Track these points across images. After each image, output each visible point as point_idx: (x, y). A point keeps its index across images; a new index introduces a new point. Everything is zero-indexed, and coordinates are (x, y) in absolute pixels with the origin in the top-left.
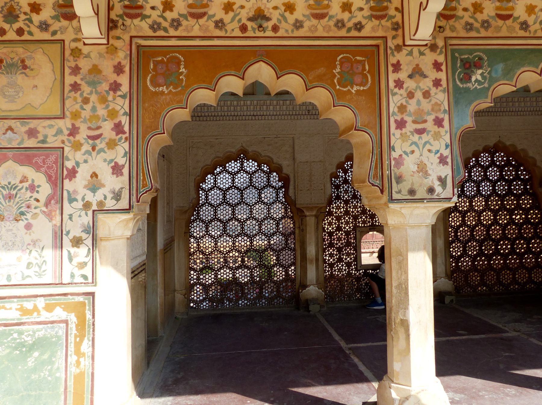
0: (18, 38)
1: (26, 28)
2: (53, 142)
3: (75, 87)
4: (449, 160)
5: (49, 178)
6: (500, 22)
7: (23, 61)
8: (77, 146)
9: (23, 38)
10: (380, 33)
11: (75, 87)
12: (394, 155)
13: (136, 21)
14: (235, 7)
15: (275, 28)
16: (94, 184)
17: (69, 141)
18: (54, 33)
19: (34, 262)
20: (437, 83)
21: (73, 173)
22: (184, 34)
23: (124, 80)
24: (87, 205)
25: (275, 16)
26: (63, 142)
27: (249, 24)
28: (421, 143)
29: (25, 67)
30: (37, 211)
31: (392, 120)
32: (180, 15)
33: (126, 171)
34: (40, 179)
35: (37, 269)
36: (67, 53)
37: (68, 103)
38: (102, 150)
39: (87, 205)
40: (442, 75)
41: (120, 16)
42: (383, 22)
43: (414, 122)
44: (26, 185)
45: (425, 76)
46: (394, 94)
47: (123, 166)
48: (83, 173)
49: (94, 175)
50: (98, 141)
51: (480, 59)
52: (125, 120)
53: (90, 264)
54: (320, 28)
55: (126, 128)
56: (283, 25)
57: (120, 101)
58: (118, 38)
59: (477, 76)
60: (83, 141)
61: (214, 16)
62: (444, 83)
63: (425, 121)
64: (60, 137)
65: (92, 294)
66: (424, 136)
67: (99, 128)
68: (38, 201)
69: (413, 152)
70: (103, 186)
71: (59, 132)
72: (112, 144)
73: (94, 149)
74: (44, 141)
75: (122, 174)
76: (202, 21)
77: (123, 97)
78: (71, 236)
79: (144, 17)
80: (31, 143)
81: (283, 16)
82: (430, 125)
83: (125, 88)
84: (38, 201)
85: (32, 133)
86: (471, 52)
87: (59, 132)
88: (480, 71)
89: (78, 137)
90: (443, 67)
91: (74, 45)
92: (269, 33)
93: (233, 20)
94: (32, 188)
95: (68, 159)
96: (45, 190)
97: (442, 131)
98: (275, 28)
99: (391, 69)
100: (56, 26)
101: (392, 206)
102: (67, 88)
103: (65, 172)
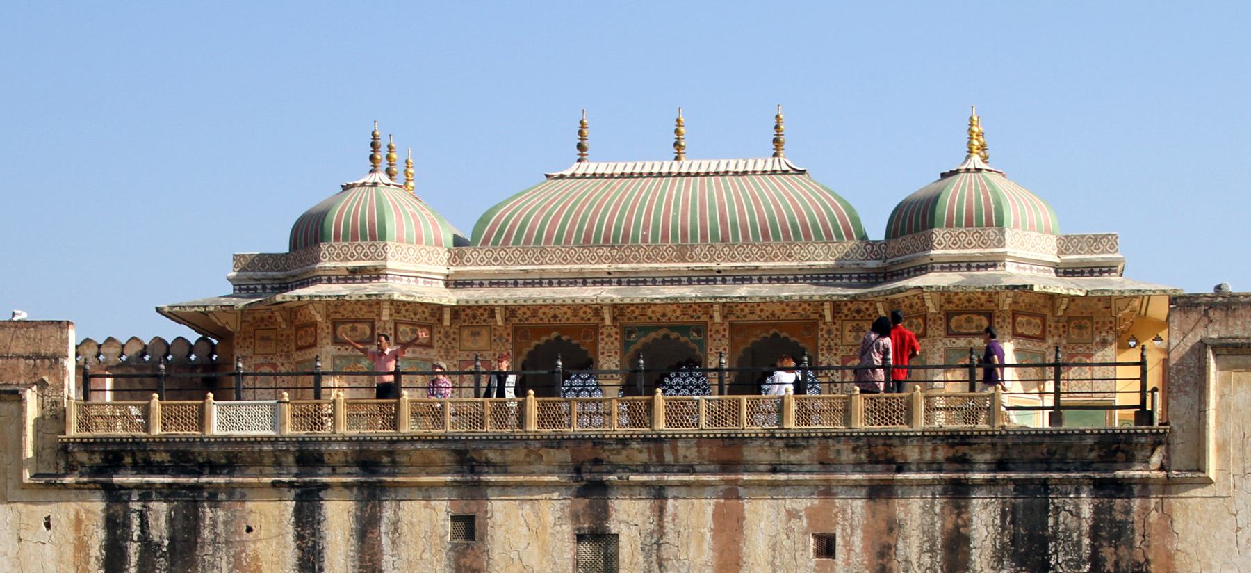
23: (510, 338)
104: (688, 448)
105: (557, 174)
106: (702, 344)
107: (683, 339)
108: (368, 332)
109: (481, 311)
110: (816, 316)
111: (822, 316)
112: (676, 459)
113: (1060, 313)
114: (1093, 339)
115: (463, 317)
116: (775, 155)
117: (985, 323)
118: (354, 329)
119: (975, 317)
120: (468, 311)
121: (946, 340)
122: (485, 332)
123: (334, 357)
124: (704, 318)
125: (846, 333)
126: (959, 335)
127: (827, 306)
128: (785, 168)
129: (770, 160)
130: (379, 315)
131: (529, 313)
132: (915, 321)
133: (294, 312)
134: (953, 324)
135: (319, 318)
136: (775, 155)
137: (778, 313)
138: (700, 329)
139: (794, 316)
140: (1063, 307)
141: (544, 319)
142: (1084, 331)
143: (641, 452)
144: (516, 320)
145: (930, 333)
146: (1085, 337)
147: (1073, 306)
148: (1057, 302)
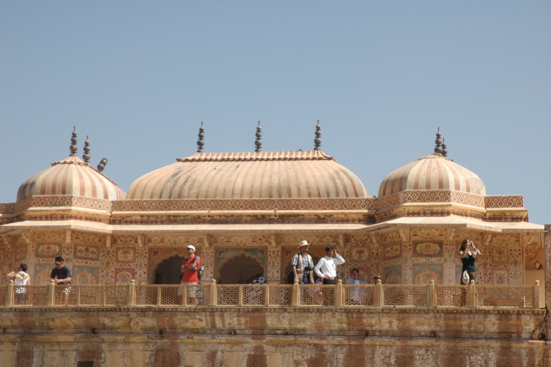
2: (133, 267)
3: (138, 257)
8: (137, 268)
20: (212, 256)
21: (136, 274)
23: (147, 255)
25: (178, 242)
40: (213, 255)
52: (147, 263)
59: (222, 254)
72: (144, 268)
80: (129, 267)
82: (209, 265)
85: (129, 265)
104: (231, 319)
105: (184, 159)
106: (265, 259)
107: (253, 257)
108: (58, 250)
109: (130, 238)
110: (335, 244)
111: (338, 243)
112: (224, 325)
113: (487, 244)
114: (508, 260)
115: (119, 242)
116: (315, 149)
117: (437, 248)
118: (49, 248)
119: (432, 245)
120: (122, 238)
121: (414, 259)
122: (131, 251)
123: (36, 265)
124: (266, 244)
126: (421, 255)
127: (341, 237)
128: (321, 156)
129: (311, 152)
130: (65, 239)
131: (159, 240)
132: (395, 247)
133: (15, 238)
134: (418, 248)
135: (28, 241)
136: (315, 149)
138: (263, 250)
139: (321, 244)
140: (489, 240)
141: (167, 243)
142: (502, 255)
143: (201, 320)
144: (151, 244)
145: (403, 255)
146: (503, 259)
147: (495, 240)
148: (485, 236)
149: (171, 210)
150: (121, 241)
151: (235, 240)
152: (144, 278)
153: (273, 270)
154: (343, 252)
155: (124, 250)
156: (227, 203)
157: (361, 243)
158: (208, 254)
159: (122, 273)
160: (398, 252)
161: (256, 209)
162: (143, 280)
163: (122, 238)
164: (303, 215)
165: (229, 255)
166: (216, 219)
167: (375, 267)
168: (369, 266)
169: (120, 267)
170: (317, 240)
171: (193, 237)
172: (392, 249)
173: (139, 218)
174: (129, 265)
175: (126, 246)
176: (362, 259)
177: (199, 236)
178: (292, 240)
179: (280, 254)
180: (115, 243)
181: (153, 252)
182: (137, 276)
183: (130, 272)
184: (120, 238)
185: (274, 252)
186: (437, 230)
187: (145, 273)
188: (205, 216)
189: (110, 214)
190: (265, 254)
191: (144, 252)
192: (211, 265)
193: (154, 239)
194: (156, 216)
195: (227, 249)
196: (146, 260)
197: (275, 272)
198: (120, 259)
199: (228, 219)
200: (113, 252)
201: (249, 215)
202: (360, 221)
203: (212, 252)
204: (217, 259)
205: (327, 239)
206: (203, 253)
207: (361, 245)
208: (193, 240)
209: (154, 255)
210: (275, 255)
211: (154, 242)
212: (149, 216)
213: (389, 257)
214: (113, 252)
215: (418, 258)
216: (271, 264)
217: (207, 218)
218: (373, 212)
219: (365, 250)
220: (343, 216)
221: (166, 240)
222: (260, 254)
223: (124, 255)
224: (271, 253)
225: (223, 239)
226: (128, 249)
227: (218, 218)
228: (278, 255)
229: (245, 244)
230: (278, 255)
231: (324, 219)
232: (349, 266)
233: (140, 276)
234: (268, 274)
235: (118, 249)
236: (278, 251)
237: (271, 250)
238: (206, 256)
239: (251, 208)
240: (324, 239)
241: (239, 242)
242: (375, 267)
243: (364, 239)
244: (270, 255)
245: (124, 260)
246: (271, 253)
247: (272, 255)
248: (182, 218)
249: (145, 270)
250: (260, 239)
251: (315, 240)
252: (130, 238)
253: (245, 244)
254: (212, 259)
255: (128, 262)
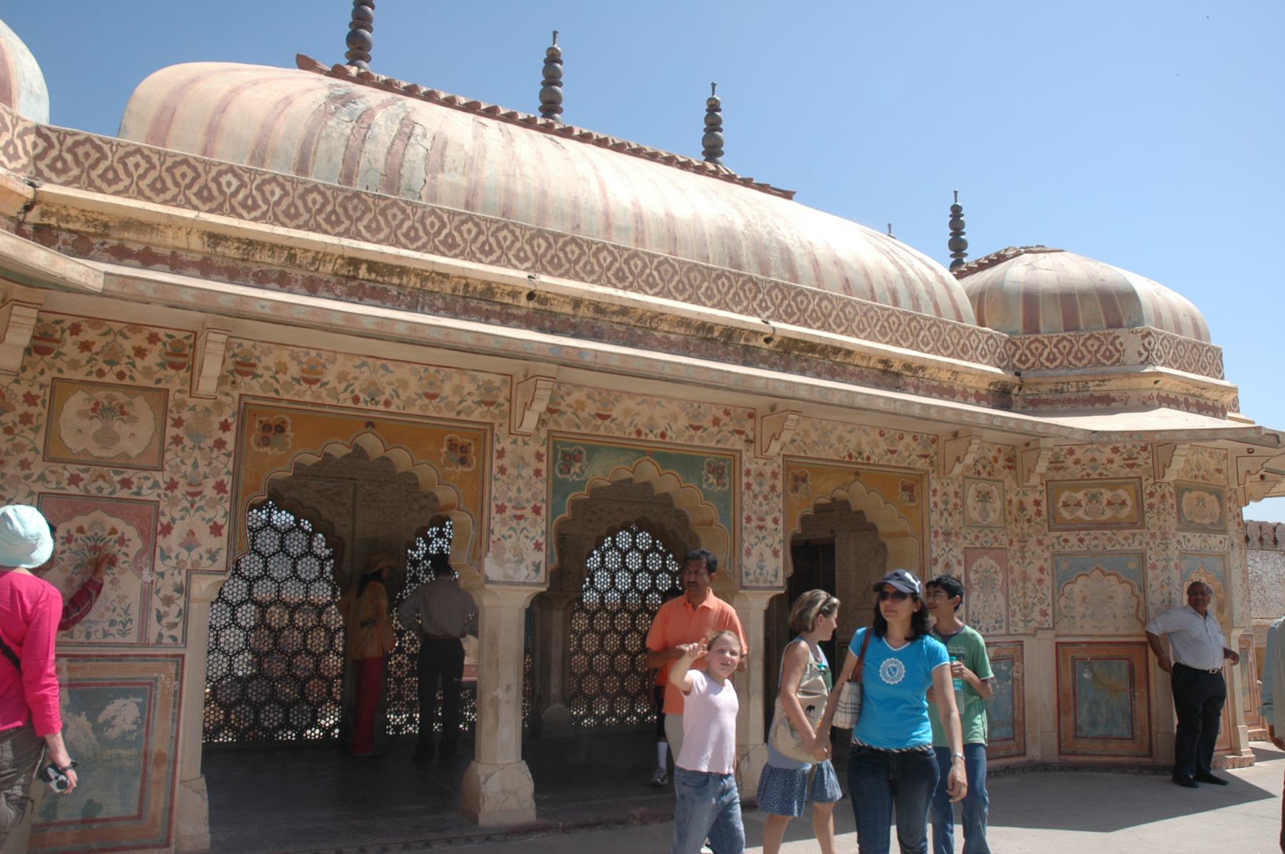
0: (119, 382)
1: (128, 373)
2: (148, 494)
3: (177, 440)
4: (544, 547)
5: (142, 534)
6: (599, 422)
7: (121, 407)
8: (174, 503)
9: (123, 382)
10: (488, 420)
11: (177, 440)
12: (493, 538)
13: (247, 379)
14: (350, 377)
15: (387, 403)
16: (190, 542)
17: (166, 495)
18: (158, 381)
19: (118, 619)
20: (538, 473)
21: (167, 530)
22: (296, 398)
23: (229, 437)
24: (180, 564)
25: (388, 391)
26: (159, 496)
27: (362, 396)
28: (518, 529)
29: (123, 413)
30: (126, 566)
31: (493, 504)
32: (293, 379)
33: (225, 531)
34: (130, 532)
35: (121, 627)
36: (171, 404)
37: (168, 456)
38: (200, 508)
39: (180, 564)
40: (543, 466)
41: (231, 372)
42: (492, 409)
43: (514, 508)
44: (115, 537)
45: (528, 465)
46: (497, 480)
47: (222, 527)
48: (179, 531)
49: (191, 533)
50: (197, 499)
51: (580, 452)
53: (181, 625)
54: (431, 407)
55: (229, 488)
56: (395, 401)
57: (223, 459)
58: (227, 394)
59: (576, 468)
60: (180, 496)
61: (327, 383)
62: (544, 473)
63: (524, 508)
64: (157, 491)
65: (183, 656)
66: (522, 522)
67: (200, 484)
68: (127, 555)
69: (510, 537)
70: (200, 545)
71: (156, 485)
72: (213, 504)
73: (192, 506)
74: (138, 493)
75: (220, 535)
76: (315, 387)
77: (228, 455)
78: (161, 594)
79: (256, 376)
80: (124, 493)
81: (395, 391)
82: (528, 512)
83: (230, 446)
84: (127, 555)
85: (126, 483)
86: (571, 445)
87: (156, 485)
88: (579, 464)
89: (176, 492)
90: (545, 458)
91: (178, 396)
92: (381, 407)
93: (346, 389)
94: (122, 541)
95: (164, 514)
96: (136, 544)
97: (539, 519)
98: (387, 403)
99: (495, 455)
100: (161, 374)
101: (487, 586)
102: (168, 440)
103: (159, 528)
106: (728, 502)
109: (140, 340)
115: (70, 348)
120: (88, 334)
122: (140, 406)
124: (737, 443)
125: (970, 502)
131: (294, 370)
137: (867, 449)
139: (893, 460)
141: (333, 392)
144: (252, 386)
145: (1152, 520)
149: (358, 236)
150: (85, 346)
151: (627, 412)
152: (213, 557)
153: (761, 547)
154: (945, 494)
155: (101, 395)
156: (595, 255)
157: (984, 467)
158: (521, 462)
159: (80, 520)
160: (1125, 513)
161: (698, 302)
162: (206, 564)
163: (88, 334)
164: (849, 353)
165: (600, 473)
166: (557, 314)
167: (1016, 545)
168: (1005, 541)
169: (73, 490)
170: (883, 445)
171: (456, 378)
172: (1094, 498)
173: (196, 243)
174: (126, 483)
175: (111, 378)
176: (989, 520)
177: (482, 377)
178: (814, 436)
179: (779, 483)
180: (42, 351)
181: (263, 423)
182: (172, 542)
183: (129, 521)
184: (75, 329)
185: (760, 475)
186: (1115, 450)
187: (216, 530)
188: (514, 294)
189: (28, 192)
190: (727, 480)
191: (216, 420)
192: (536, 510)
193: (269, 361)
194: (290, 252)
195: (594, 449)
196: (224, 465)
197: (768, 553)
198: (71, 442)
199: (604, 321)
200: (30, 399)
201: (685, 322)
202: (979, 399)
203: (539, 456)
204: (558, 488)
205: (907, 447)
206: (501, 454)
207: (984, 475)
208: (458, 389)
209: (266, 442)
210: (766, 488)
211: (267, 375)
212: (251, 244)
213: (1078, 520)
214: (30, 399)
215: (1188, 535)
216: (754, 523)
217: (523, 301)
218: (1009, 377)
219: (995, 493)
220: (945, 376)
221: (330, 376)
222: (712, 479)
223: (97, 425)
224: (751, 480)
225: (580, 405)
226: (121, 397)
227: (568, 309)
228: (773, 488)
229: (663, 435)
230: (773, 488)
231: (898, 375)
232: (961, 540)
233: (190, 542)
234: (745, 560)
235: (60, 388)
236: (774, 475)
237: (753, 467)
238: (511, 471)
239: (681, 292)
240: (900, 446)
241: (641, 422)
242: (1016, 545)
243: (990, 456)
244: (749, 486)
245: (97, 452)
246: (751, 480)
247: (755, 487)
248: (414, 282)
249: (219, 514)
250: (716, 422)
251: (876, 444)
252: (140, 340)
253: (663, 435)
254: (541, 486)
255: (123, 464)
